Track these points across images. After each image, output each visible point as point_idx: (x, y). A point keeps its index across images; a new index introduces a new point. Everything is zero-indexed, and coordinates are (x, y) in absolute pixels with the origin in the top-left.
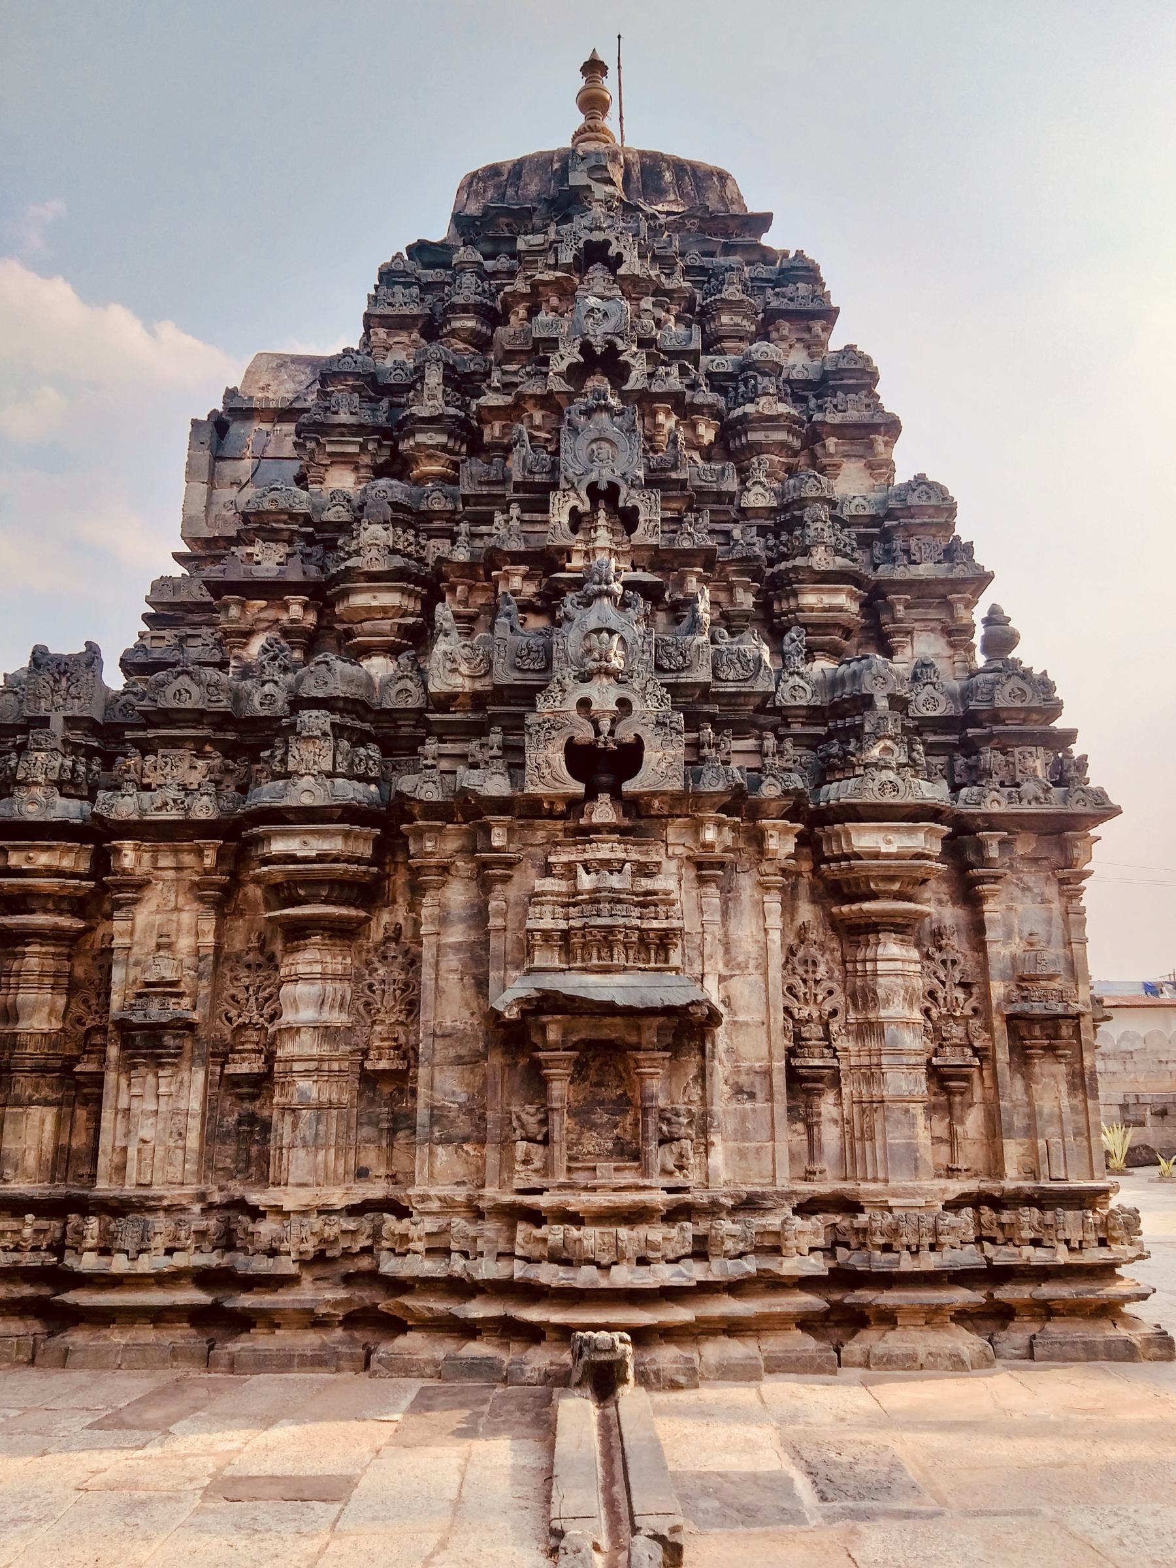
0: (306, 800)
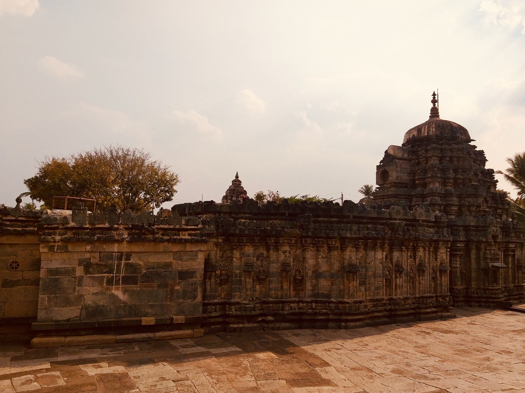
0: (462, 240)
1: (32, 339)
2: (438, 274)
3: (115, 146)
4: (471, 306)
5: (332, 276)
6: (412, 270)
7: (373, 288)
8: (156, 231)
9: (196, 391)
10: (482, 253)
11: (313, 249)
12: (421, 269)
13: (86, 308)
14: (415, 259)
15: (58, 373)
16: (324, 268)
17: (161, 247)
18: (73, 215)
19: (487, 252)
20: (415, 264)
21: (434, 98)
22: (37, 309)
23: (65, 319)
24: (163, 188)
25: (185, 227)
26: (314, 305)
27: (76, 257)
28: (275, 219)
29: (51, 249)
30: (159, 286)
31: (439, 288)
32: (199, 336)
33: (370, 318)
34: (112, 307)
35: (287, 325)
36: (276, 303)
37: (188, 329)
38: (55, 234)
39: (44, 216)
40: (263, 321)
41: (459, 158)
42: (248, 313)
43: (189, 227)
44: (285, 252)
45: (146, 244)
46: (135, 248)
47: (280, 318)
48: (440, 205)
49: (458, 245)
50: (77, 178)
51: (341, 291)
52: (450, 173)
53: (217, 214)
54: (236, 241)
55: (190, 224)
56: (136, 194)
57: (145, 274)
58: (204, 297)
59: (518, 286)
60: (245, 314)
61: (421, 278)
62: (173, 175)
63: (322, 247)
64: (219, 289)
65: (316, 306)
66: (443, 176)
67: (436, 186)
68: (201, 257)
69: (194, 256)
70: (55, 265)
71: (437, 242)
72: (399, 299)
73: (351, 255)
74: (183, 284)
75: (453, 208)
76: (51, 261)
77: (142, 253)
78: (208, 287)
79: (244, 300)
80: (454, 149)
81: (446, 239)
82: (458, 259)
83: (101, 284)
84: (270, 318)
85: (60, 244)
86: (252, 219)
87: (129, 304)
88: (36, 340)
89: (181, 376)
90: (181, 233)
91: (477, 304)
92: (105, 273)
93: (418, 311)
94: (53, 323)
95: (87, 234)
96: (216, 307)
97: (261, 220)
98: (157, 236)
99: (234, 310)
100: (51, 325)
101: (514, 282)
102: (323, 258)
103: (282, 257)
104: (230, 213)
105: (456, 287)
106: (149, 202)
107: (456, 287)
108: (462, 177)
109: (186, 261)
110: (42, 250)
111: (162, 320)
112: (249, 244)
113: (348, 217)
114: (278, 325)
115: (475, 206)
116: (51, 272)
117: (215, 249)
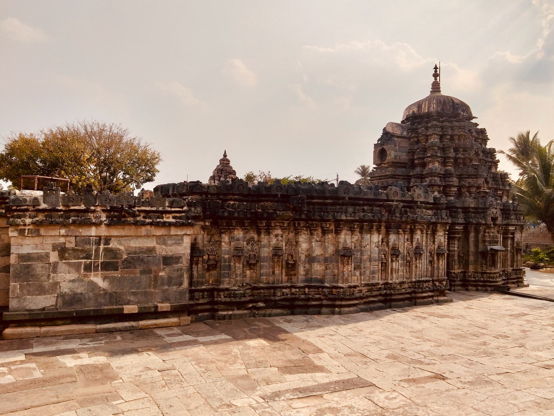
1: (4, 329)
2: (436, 258)
3: (89, 121)
4: (467, 290)
5: (326, 260)
6: (409, 253)
7: (368, 272)
8: (137, 213)
9: (184, 380)
10: (480, 236)
11: (306, 232)
13: (62, 296)
14: (412, 242)
15: (33, 365)
16: (318, 251)
17: (143, 230)
18: (45, 196)
19: (486, 234)
21: (436, 71)
22: (8, 297)
23: (39, 308)
24: (144, 167)
25: (169, 209)
26: (307, 290)
27: (50, 241)
28: (267, 201)
29: (22, 233)
30: (142, 273)
31: (436, 272)
32: (186, 324)
33: (365, 303)
34: (91, 294)
35: (279, 311)
36: (267, 288)
37: (173, 317)
38: (25, 216)
39: (12, 197)
40: (254, 308)
41: (459, 136)
42: (238, 300)
43: (173, 209)
44: (276, 236)
45: (127, 227)
46: (114, 232)
47: (272, 304)
48: (439, 186)
49: (456, 228)
50: (47, 156)
51: (334, 275)
52: (450, 152)
53: (204, 196)
54: (225, 225)
55: (175, 205)
56: (114, 174)
57: (125, 260)
58: (191, 283)
59: (517, 270)
60: (234, 301)
61: (418, 261)
62: (154, 153)
63: (315, 230)
64: (207, 275)
65: (309, 292)
66: (443, 155)
67: (436, 166)
68: (187, 241)
69: (179, 240)
70: (25, 250)
71: (435, 224)
72: (395, 283)
73: (346, 238)
74: (167, 269)
75: (452, 189)
76: (22, 246)
77: (122, 237)
78: (195, 273)
79: (234, 285)
80: (455, 126)
81: (445, 221)
82: (456, 242)
83: (78, 270)
84: (261, 304)
85: (31, 227)
86: (242, 201)
87: (109, 291)
88: (8, 331)
89: (167, 366)
90: (164, 215)
91: (474, 288)
92: (82, 259)
93: (413, 295)
94: (26, 312)
95: (61, 216)
96: (203, 294)
97: (252, 201)
98: (138, 219)
99: (222, 297)
100: (24, 315)
101: (512, 266)
102: (317, 241)
103: (274, 241)
104: (218, 194)
105: (453, 271)
106: (128, 183)
107: (453, 271)
108: (463, 157)
109: (170, 246)
110: (11, 234)
111: (145, 308)
112: (238, 228)
113: (344, 198)
114: (269, 311)
115: (475, 187)
116: (22, 257)
117: (202, 233)
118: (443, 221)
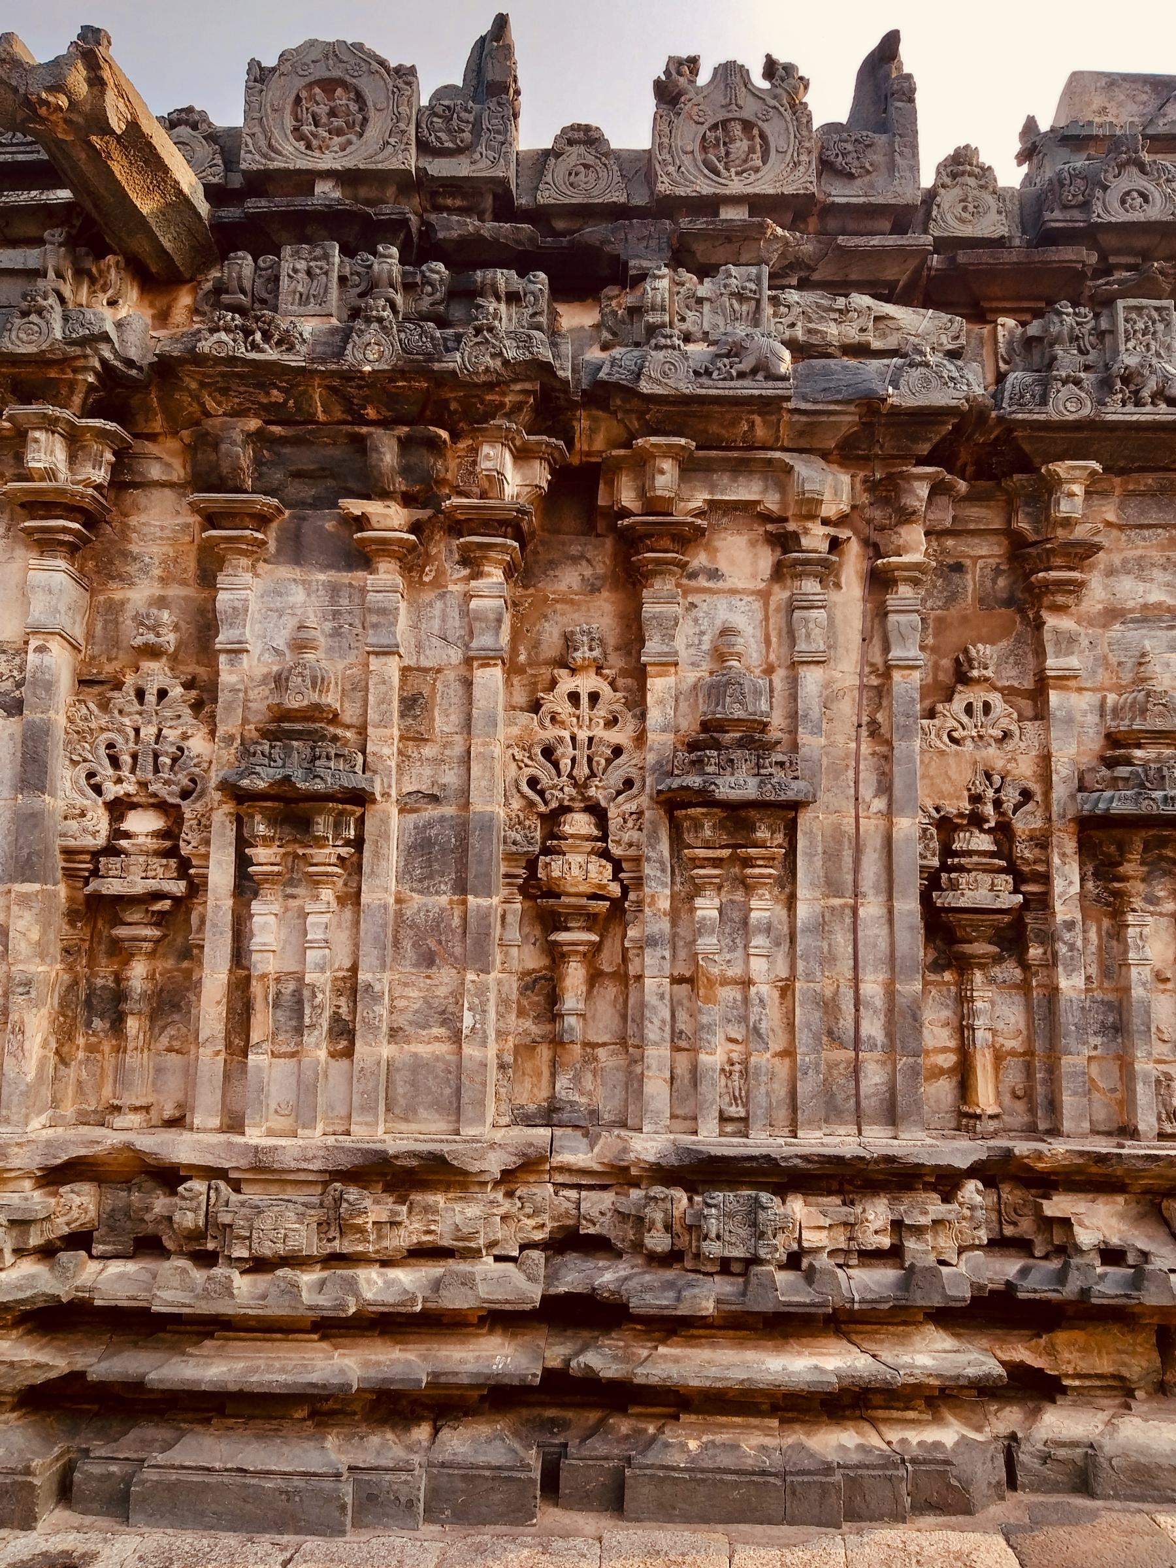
2: (1068, 881)
6: (598, 813)
12: (728, 806)
20: (640, 739)
31: (1081, 1056)
61: (707, 907)
71: (992, 456)
72: (265, 1170)
118: (1117, 412)
